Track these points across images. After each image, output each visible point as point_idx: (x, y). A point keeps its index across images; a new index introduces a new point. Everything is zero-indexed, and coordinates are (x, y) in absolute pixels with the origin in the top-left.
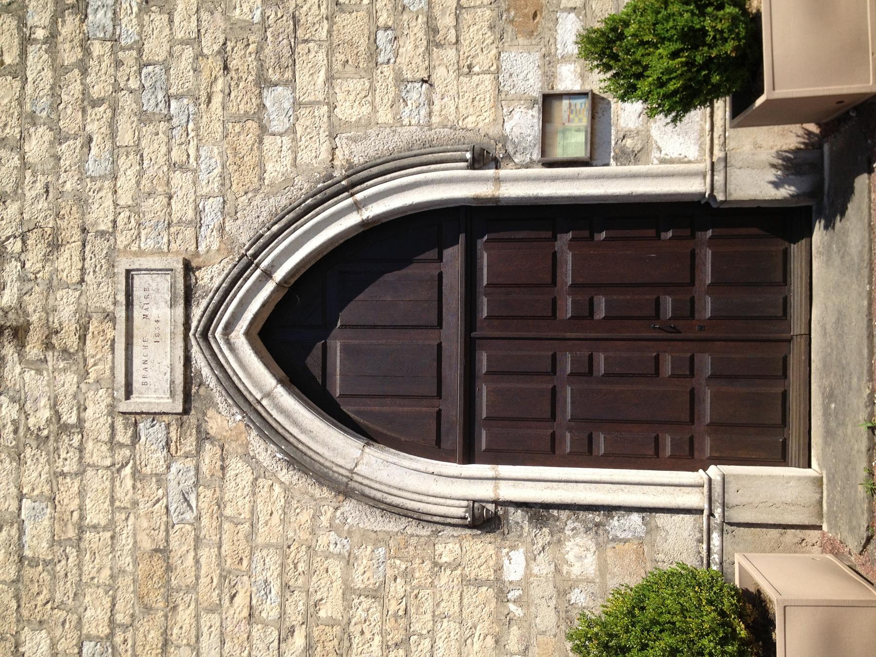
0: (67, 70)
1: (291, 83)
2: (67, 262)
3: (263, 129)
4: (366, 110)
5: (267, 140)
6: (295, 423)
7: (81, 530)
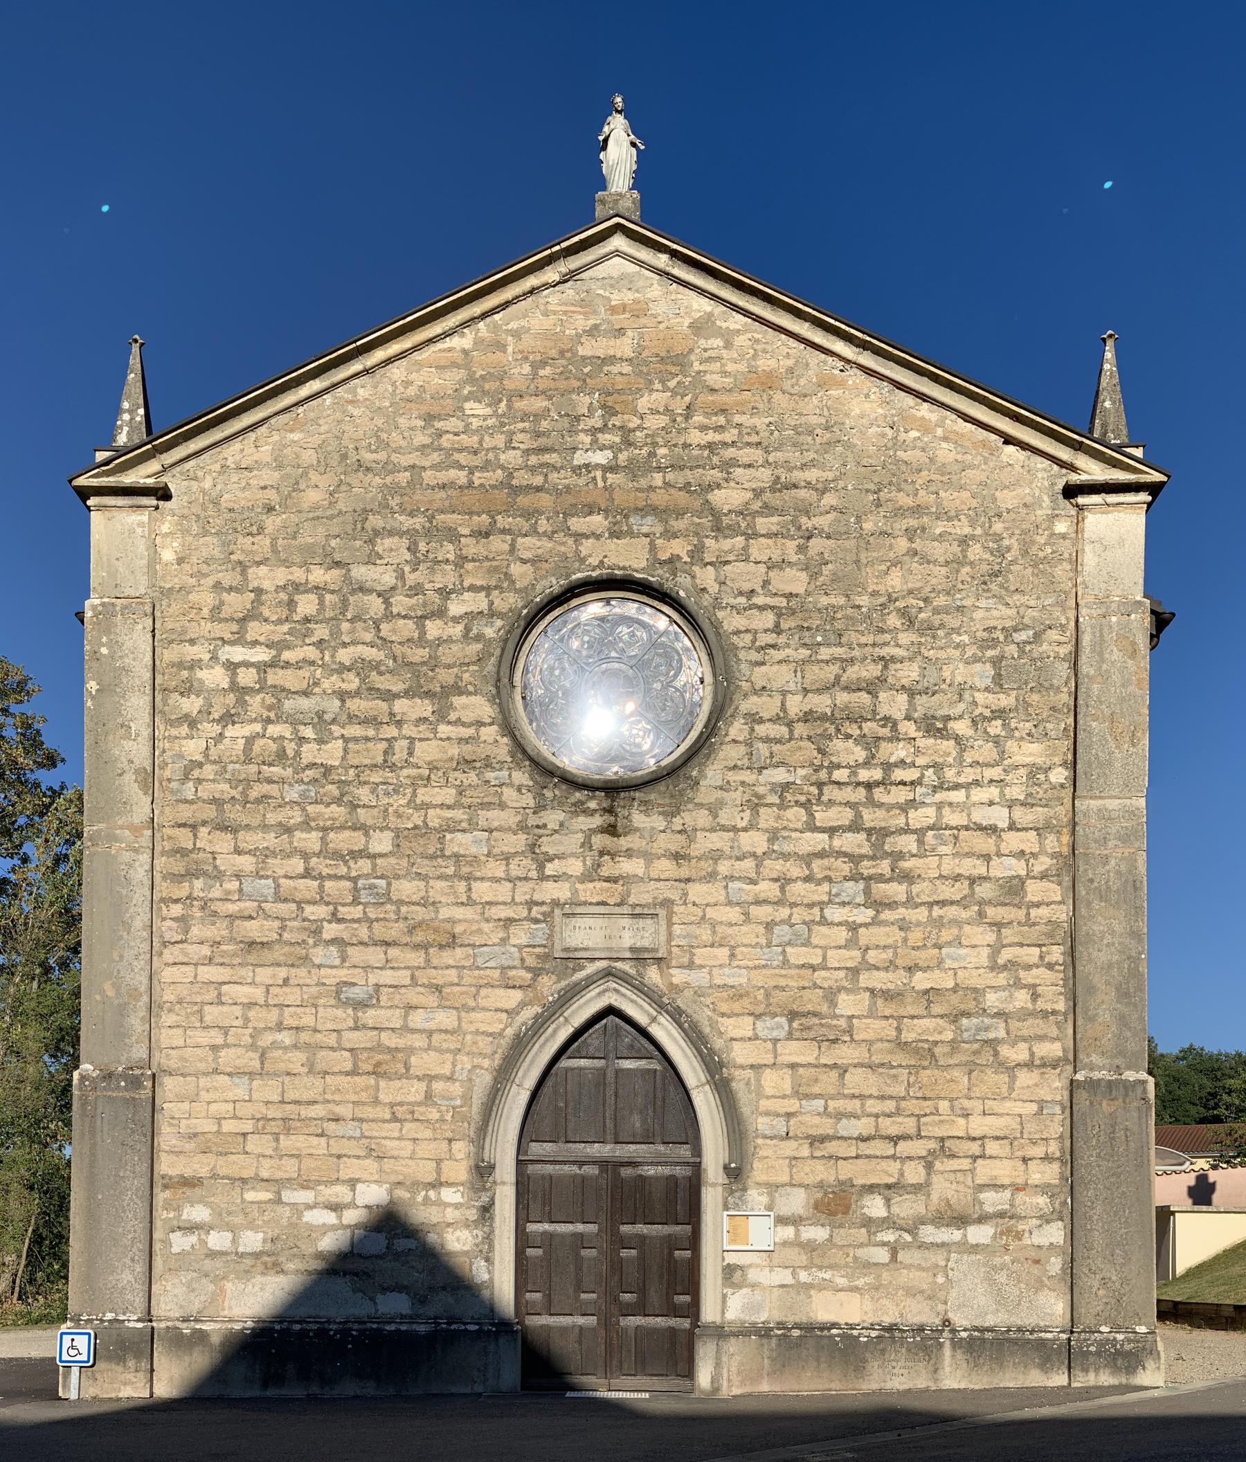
0: (808, 865)
1: (790, 1036)
2: (664, 867)
3: (758, 1016)
4: (769, 1091)
5: (750, 1019)
6: (547, 1040)
7: (468, 879)
